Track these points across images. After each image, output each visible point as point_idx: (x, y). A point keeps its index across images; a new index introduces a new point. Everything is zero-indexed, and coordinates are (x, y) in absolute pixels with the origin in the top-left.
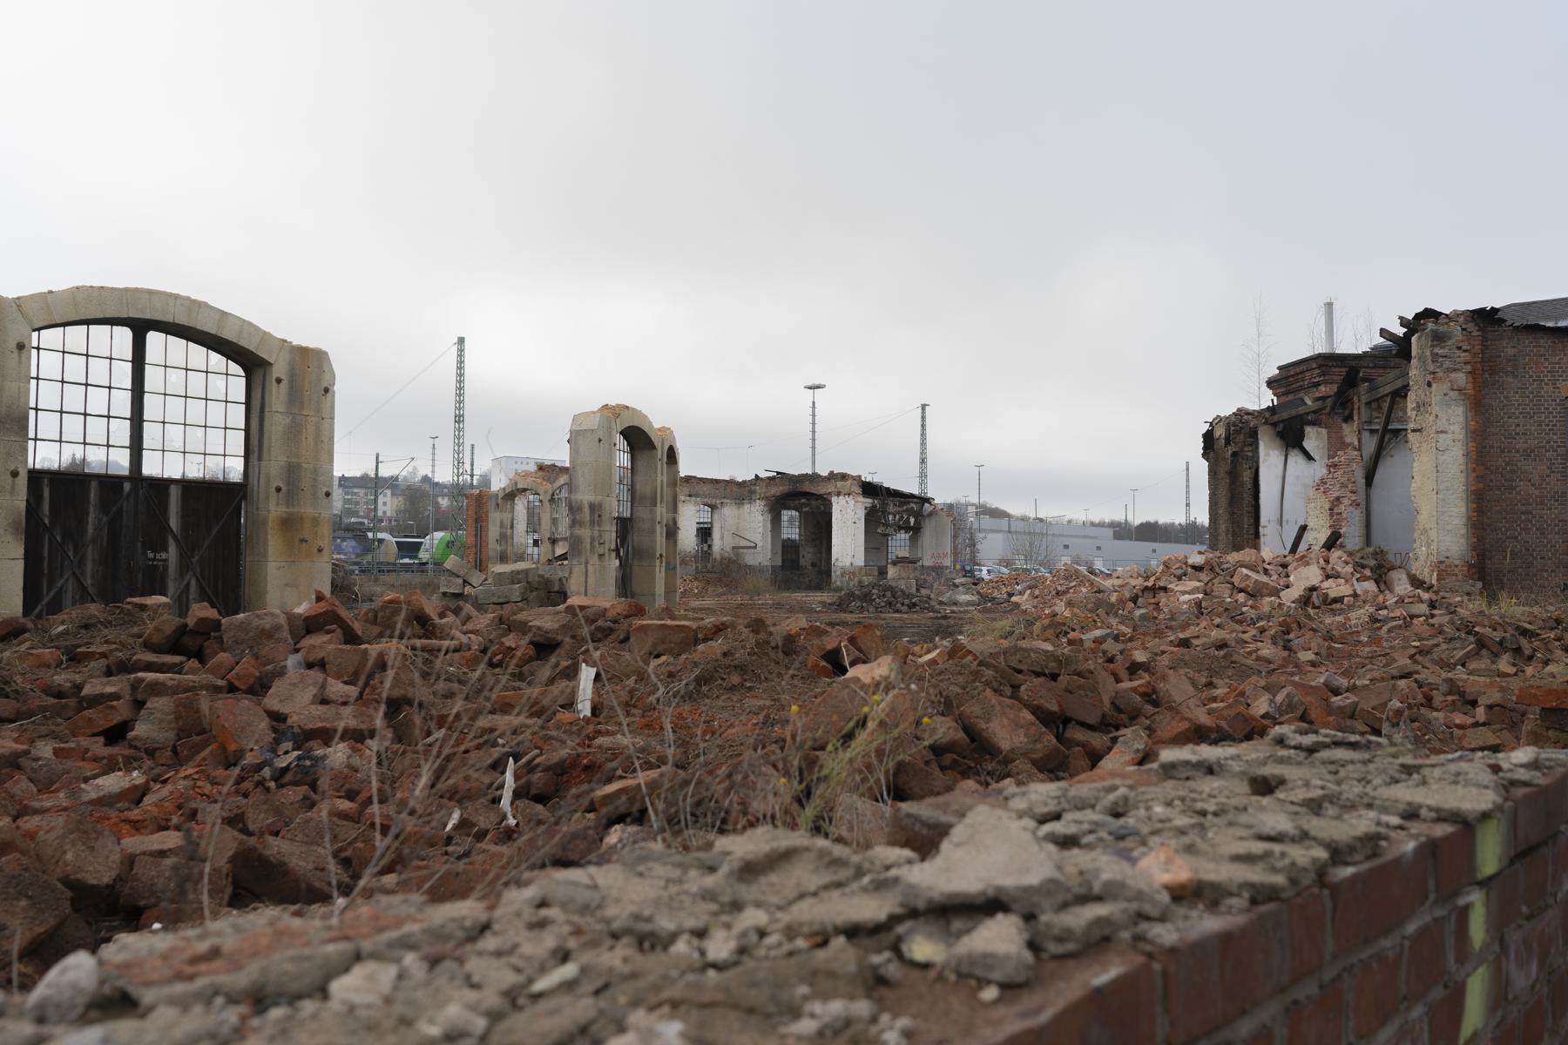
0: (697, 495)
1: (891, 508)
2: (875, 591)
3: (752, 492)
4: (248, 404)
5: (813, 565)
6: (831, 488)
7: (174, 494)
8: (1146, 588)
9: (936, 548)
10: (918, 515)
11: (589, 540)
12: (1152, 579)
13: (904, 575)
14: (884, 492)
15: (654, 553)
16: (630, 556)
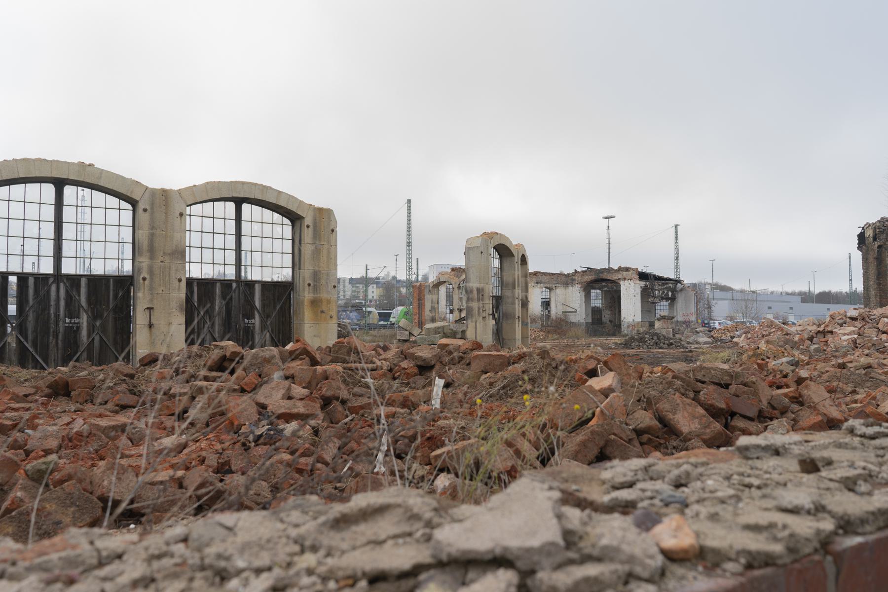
0: (541, 283)
1: (657, 287)
2: (647, 336)
3: (573, 280)
4: (293, 240)
5: (611, 321)
6: (619, 276)
7: (258, 288)
8: (819, 332)
9: (684, 310)
10: (674, 291)
11: (477, 309)
12: (823, 326)
13: (665, 326)
14: (652, 277)
15: (515, 316)
16: (501, 318)
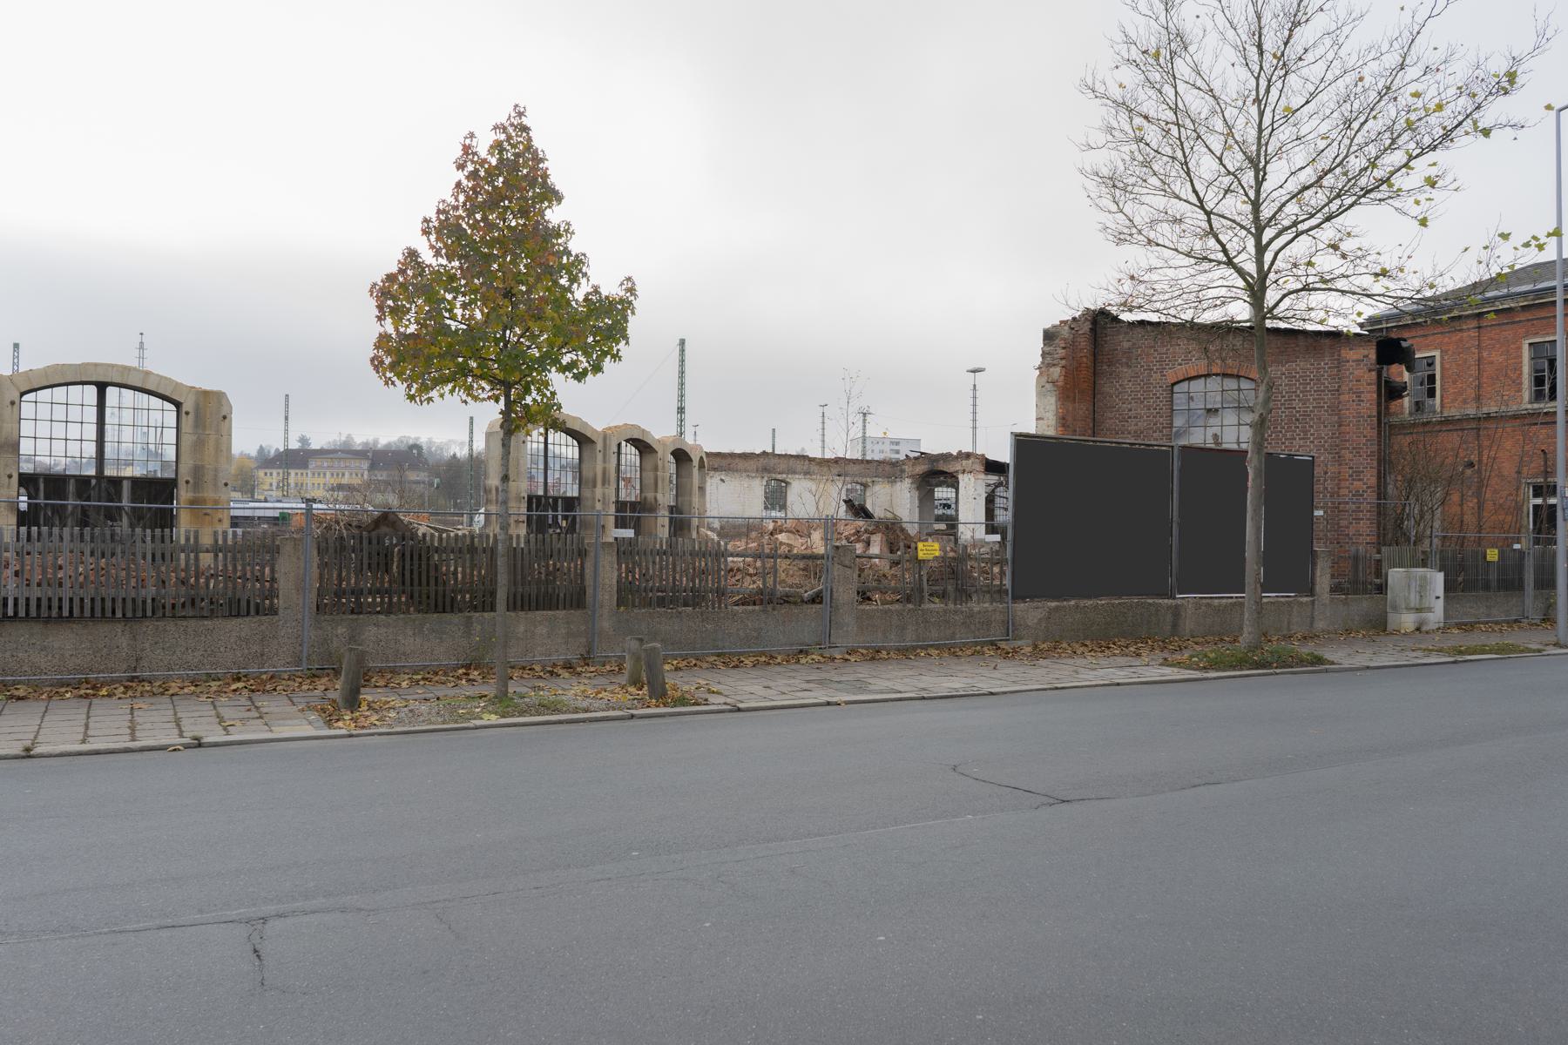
7: (126, 486)
